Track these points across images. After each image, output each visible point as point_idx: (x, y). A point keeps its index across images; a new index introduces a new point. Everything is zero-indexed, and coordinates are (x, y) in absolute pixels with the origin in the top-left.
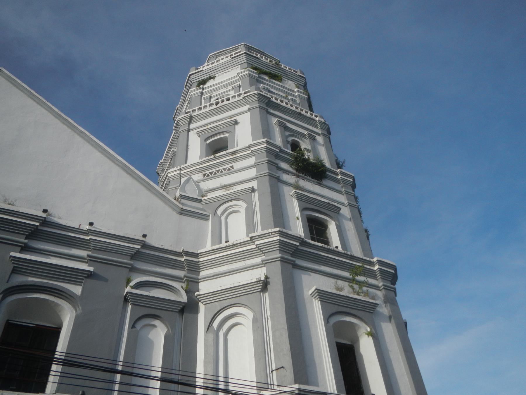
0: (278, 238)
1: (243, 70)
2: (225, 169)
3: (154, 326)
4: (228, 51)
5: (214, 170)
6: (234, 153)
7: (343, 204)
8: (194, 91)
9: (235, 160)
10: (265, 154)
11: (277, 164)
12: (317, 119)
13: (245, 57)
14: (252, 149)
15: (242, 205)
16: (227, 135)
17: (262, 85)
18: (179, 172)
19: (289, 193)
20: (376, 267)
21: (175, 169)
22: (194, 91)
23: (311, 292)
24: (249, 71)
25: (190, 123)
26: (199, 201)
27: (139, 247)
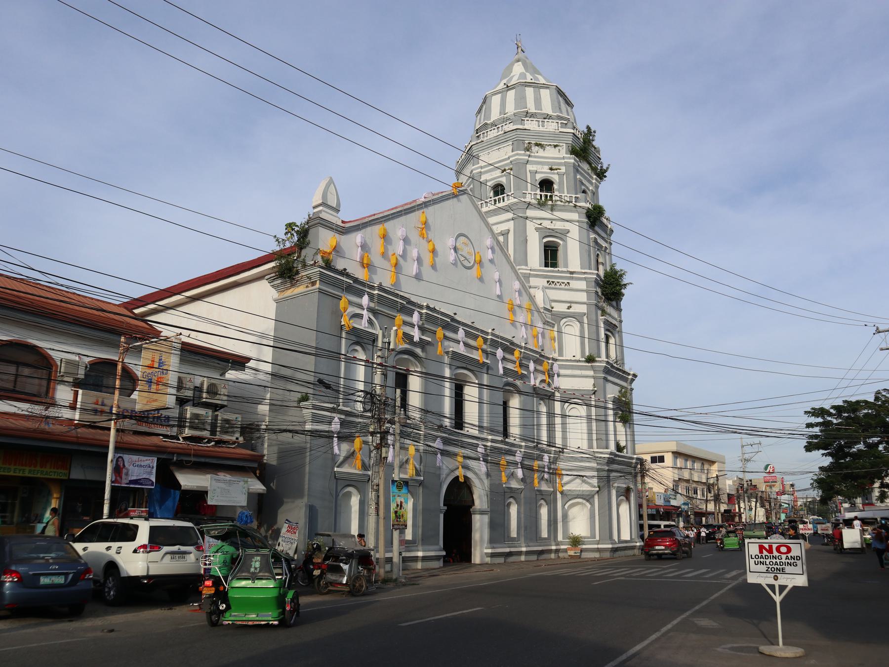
0: (605, 365)
1: (569, 156)
2: (563, 283)
3: (540, 404)
4: (539, 85)
5: (556, 281)
6: (572, 273)
7: (616, 320)
8: (520, 155)
9: (572, 278)
10: (593, 284)
11: (598, 293)
12: (609, 226)
13: (572, 137)
14: (586, 276)
15: (577, 325)
16: (561, 242)
17: (578, 177)
18: (529, 272)
19: (601, 318)
20: (630, 377)
21: (526, 268)
22: (520, 155)
23: (609, 396)
24: (575, 160)
25: (526, 209)
26: (550, 311)
27: (538, 356)
